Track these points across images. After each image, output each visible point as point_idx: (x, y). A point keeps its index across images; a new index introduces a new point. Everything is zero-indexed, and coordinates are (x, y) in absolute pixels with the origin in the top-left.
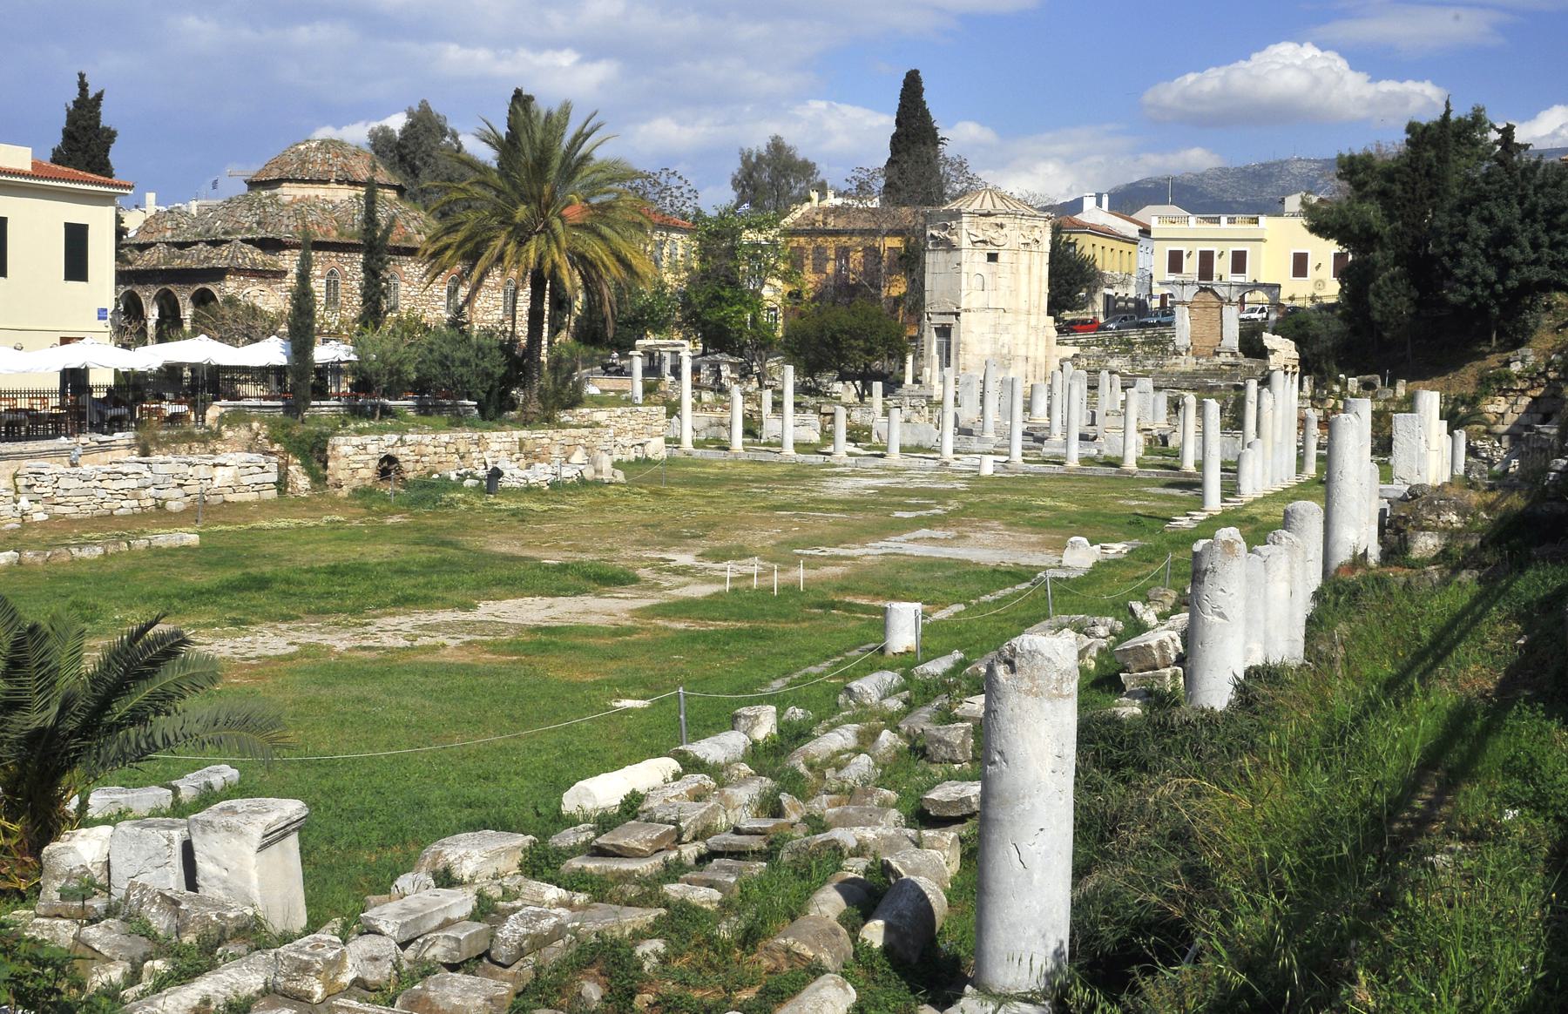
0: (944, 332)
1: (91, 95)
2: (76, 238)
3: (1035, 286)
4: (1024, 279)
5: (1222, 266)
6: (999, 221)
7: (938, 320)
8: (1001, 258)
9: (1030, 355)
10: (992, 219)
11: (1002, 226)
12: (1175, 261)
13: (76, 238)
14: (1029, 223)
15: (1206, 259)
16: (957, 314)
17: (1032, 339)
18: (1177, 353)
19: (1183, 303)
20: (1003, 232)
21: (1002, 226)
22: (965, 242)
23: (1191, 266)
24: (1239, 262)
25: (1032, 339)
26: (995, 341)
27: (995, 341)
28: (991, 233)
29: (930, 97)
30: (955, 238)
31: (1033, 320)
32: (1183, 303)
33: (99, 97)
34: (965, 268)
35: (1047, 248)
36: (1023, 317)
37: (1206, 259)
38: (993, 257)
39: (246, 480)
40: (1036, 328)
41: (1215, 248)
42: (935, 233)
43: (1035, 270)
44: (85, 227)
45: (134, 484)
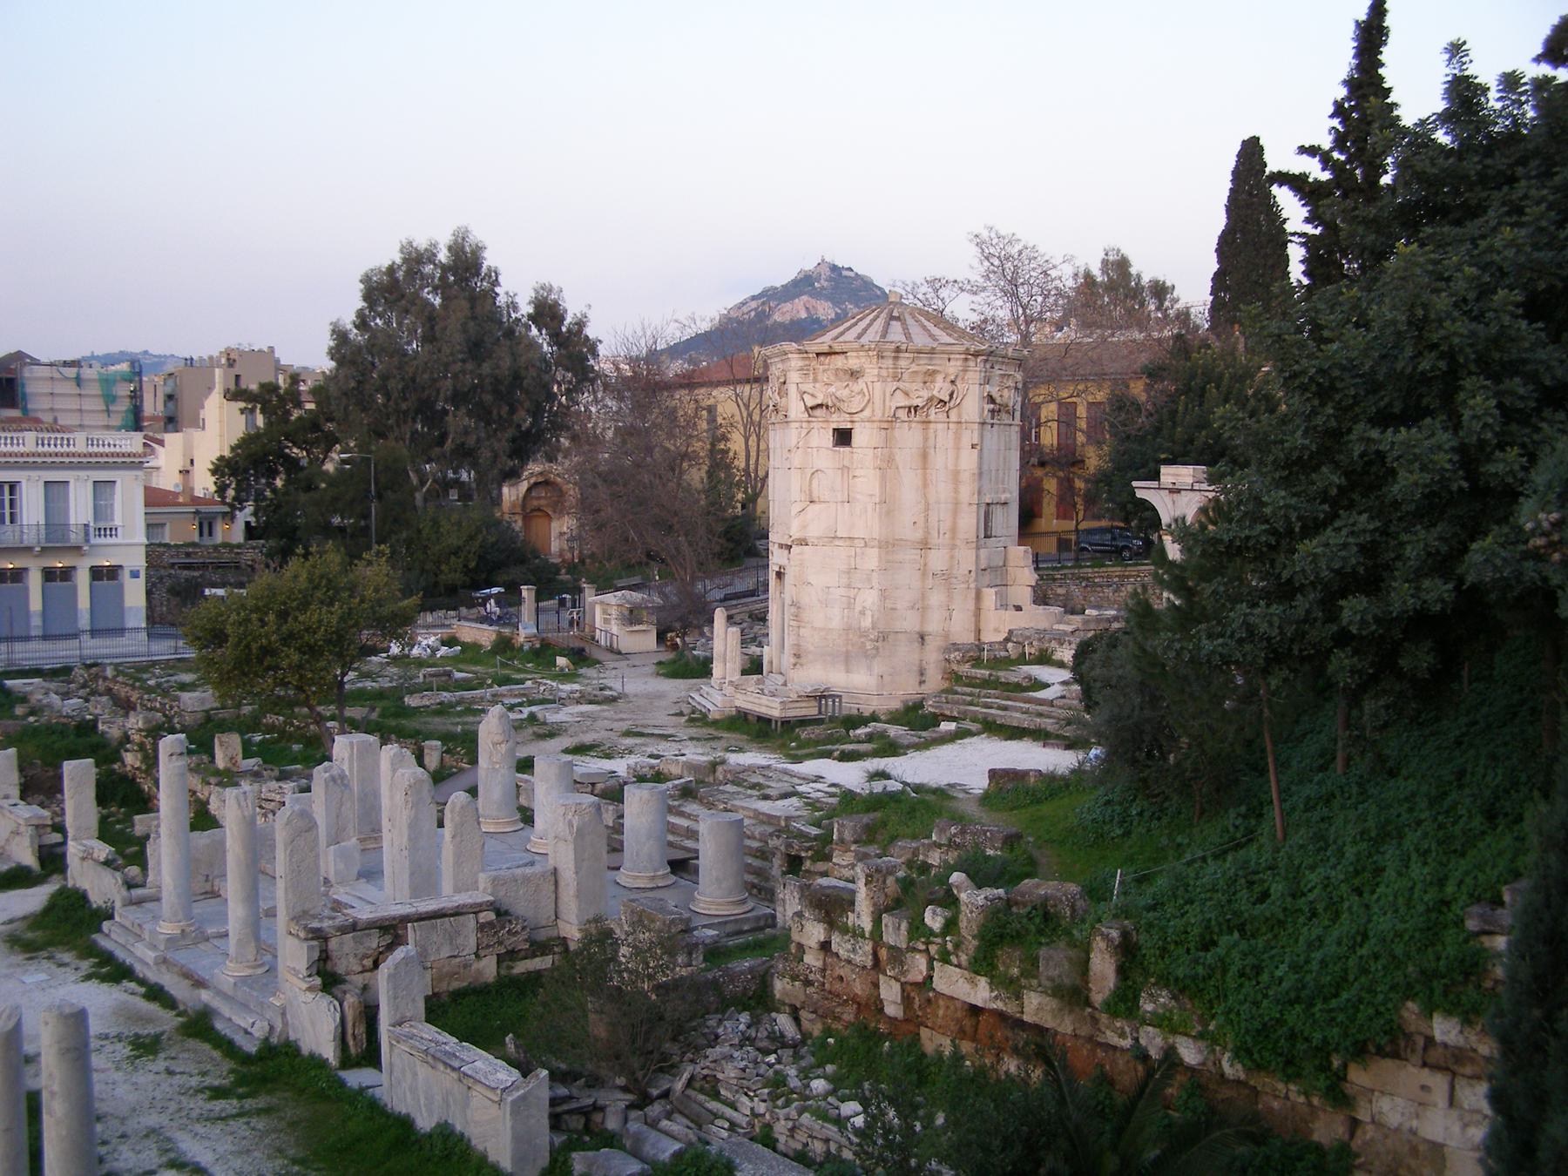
3: (941, 489)
4: (909, 479)
6: (853, 362)
8: (856, 438)
9: (934, 625)
10: (839, 361)
11: (854, 374)
14: (923, 365)
17: (936, 599)
21: (854, 374)
25: (936, 599)
26: (850, 604)
28: (840, 390)
31: (937, 560)
36: (911, 555)
38: (843, 437)
40: (947, 577)
43: (941, 461)
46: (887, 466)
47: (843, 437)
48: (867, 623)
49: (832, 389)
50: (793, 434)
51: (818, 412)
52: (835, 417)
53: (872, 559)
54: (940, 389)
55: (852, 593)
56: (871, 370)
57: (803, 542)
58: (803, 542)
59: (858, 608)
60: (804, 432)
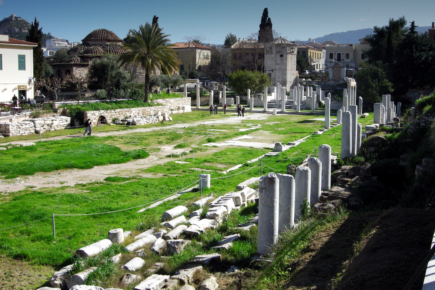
1: (37, 22)
2: (22, 59)
13: (22, 59)
15: (339, 55)
16: (273, 71)
22: (274, 51)
27: (283, 78)
29: (270, 15)
31: (293, 72)
33: (38, 22)
35: (296, 52)
37: (339, 55)
38: (282, 56)
39: (61, 124)
43: (293, 59)
44: (19, 55)
45: (28, 126)
47: (282, 56)
50: (273, 56)
57: (275, 70)
58: (275, 70)
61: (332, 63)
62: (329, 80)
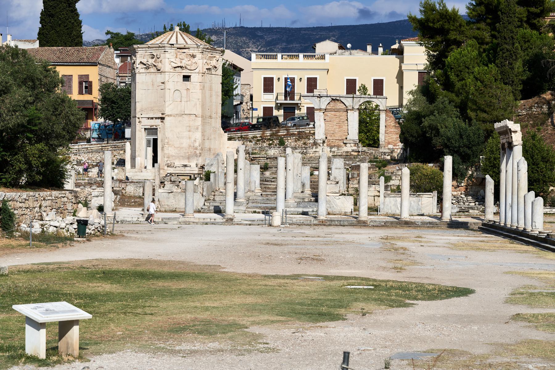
0: (152, 131)
5: (301, 88)
6: (191, 52)
7: (149, 123)
9: (212, 147)
11: (193, 56)
12: (268, 85)
15: (290, 83)
16: (163, 119)
18: (315, 144)
19: (320, 109)
20: (196, 59)
21: (193, 56)
23: (279, 87)
24: (312, 84)
30: (159, 65)
32: (320, 109)
34: (169, 85)
37: (290, 83)
38: (186, 78)
41: (296, 75)
42: (144, 61)
46: (203, 88)
47: (186, 78)
48: (197, 144)
49: (184, 61)
51: (177, 69)
52: (184, 71)
53: (199, 121)
54: (214, 63)
55: (191, 133)
56: (199, 56)
57: (168, 116)
58: (168, 116)
59: (193, 139)
60: (171, 76)
61: (323, 99)
62: (315, 144)
